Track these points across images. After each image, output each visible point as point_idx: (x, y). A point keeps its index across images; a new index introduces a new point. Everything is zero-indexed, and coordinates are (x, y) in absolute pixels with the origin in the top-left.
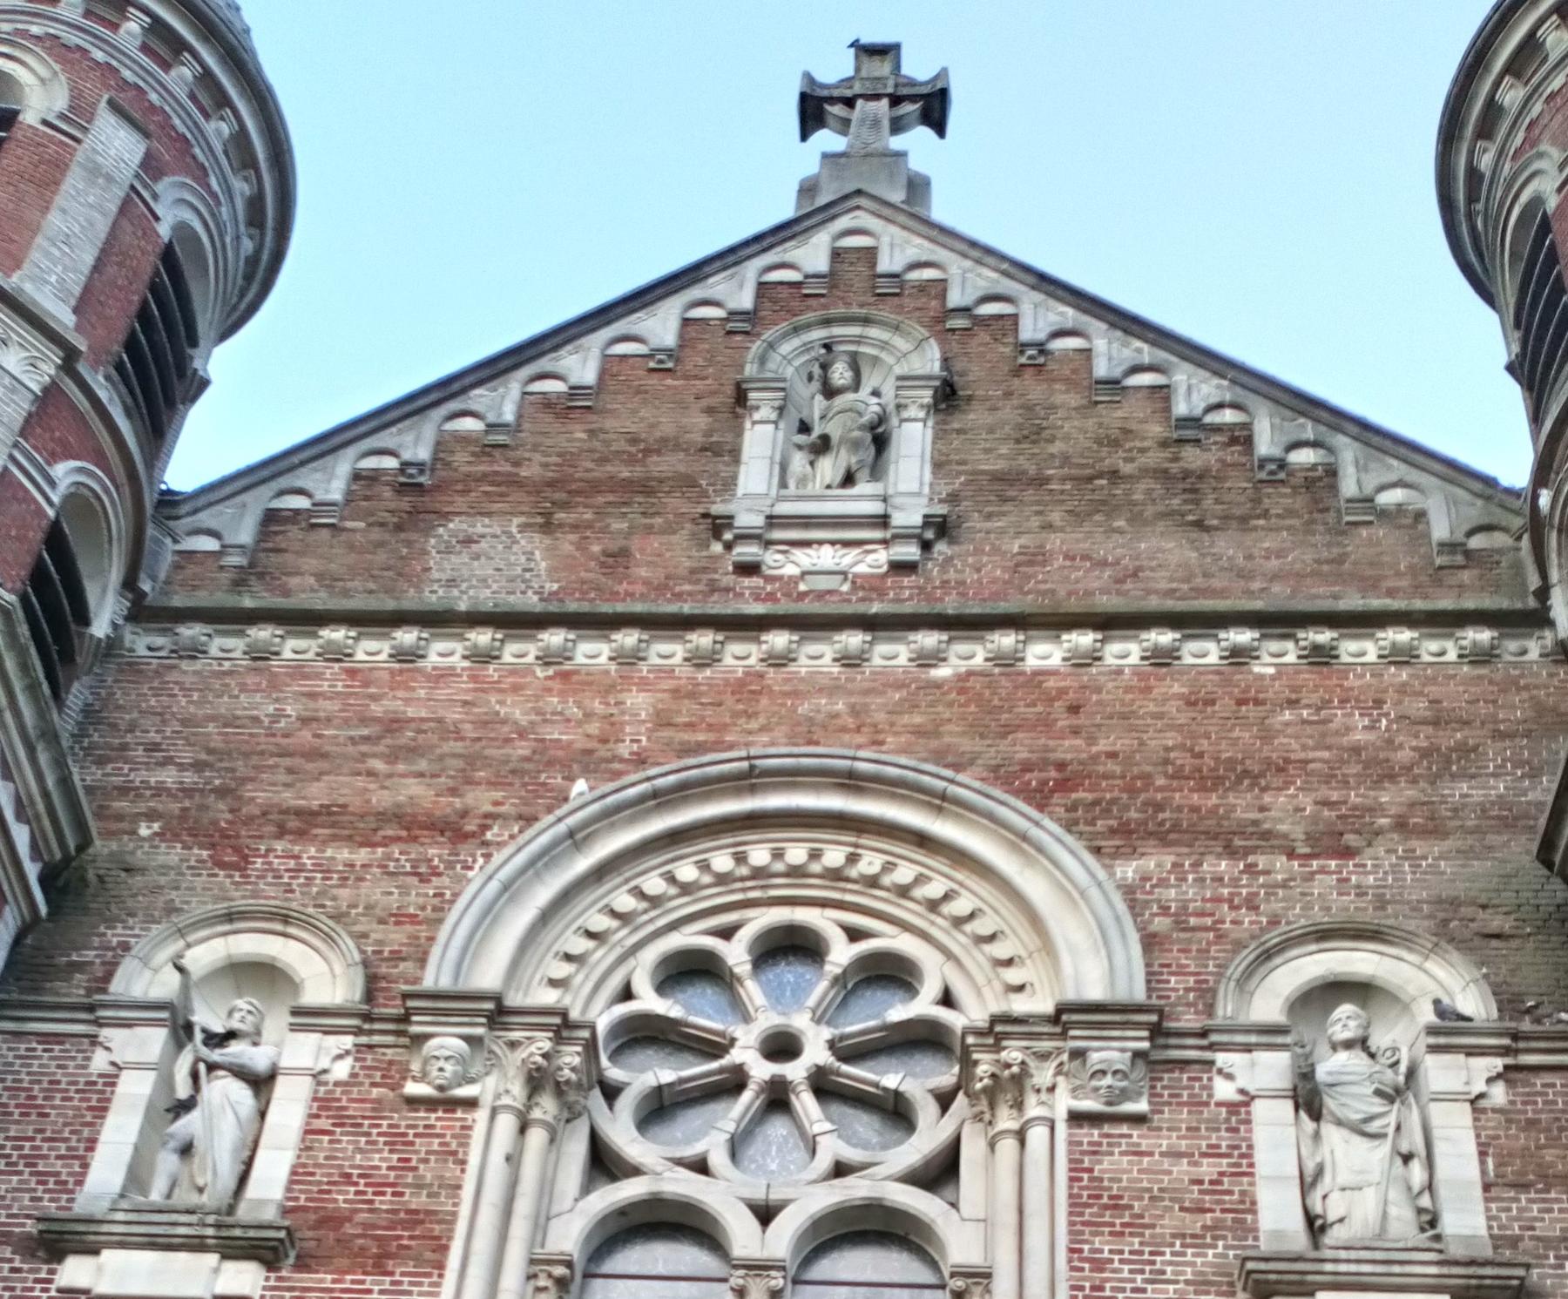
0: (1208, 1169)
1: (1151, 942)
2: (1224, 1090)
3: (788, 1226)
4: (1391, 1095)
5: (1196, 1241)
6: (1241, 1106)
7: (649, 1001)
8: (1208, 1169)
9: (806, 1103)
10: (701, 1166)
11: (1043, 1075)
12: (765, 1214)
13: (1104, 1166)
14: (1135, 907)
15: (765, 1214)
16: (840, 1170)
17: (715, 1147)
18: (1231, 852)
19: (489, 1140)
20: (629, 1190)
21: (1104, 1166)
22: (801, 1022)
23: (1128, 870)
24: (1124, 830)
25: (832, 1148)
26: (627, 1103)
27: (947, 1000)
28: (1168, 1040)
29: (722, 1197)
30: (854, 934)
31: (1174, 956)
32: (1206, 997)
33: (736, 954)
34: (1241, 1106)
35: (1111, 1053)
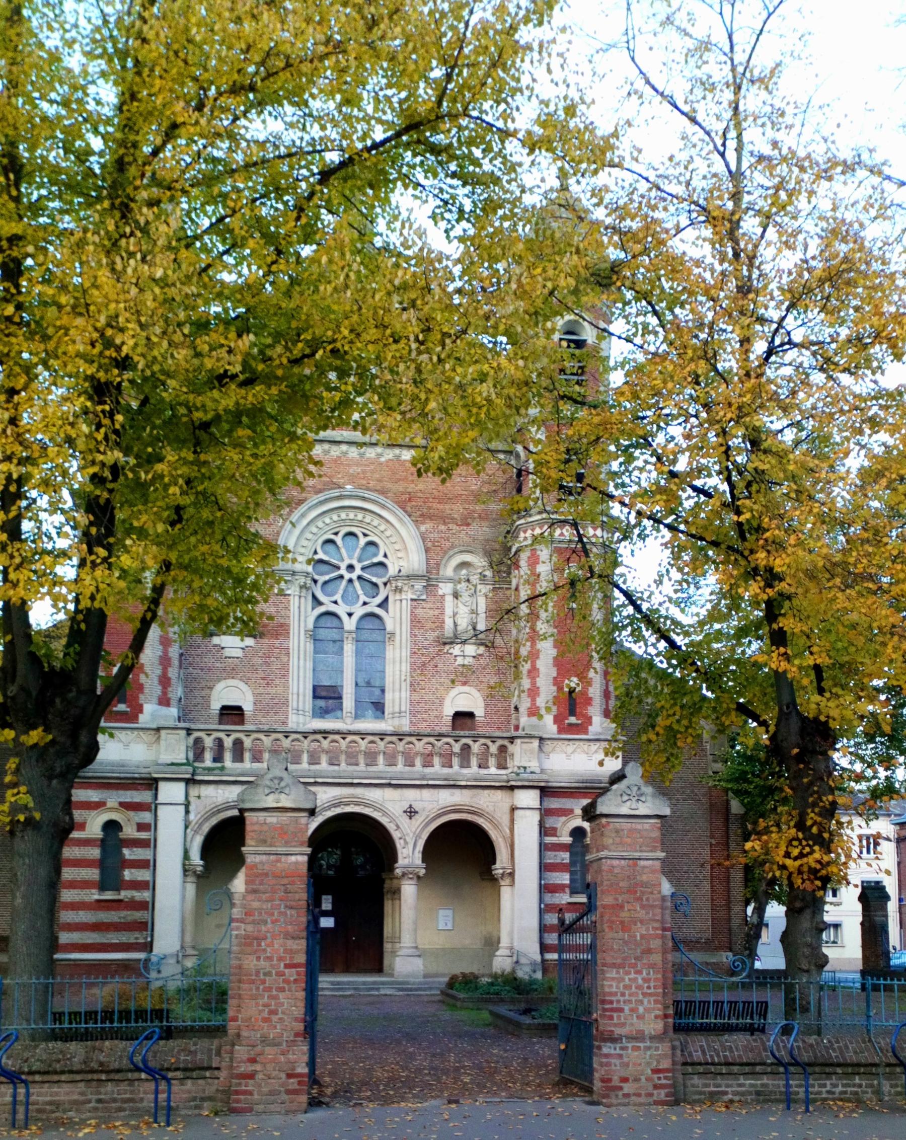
0: (437, 612)
1: (427, 550)
2: (440, 592)
3: (355, 618)
4: (471, 596)
5: (433, 630)
6: (443, 596)
7: (321, 555)
8: (437, 612)
9: (357, 584)
10: (336, 602)
11: (405, 588)
12: (350, 615)
13: (417, 611)
14: (424, 540)
15: (350, 615)
16: (365, 604)
17: (338, 597)
18: (445, 523)
19: (294, 602)
20: (322, 609)
21: (417, 611)
22: (354, 562)
23: (423, 528)
24: (422, 515)
25: (363, 598)
26: (319, 584)
27: (385, 556)
28: (429, 579)
29: (341, 610)
30: (365, 535)
31: (432, 554)
32: (438, 565)
33: (338, 539)
34: (443, 596)
35: (419, 585)
